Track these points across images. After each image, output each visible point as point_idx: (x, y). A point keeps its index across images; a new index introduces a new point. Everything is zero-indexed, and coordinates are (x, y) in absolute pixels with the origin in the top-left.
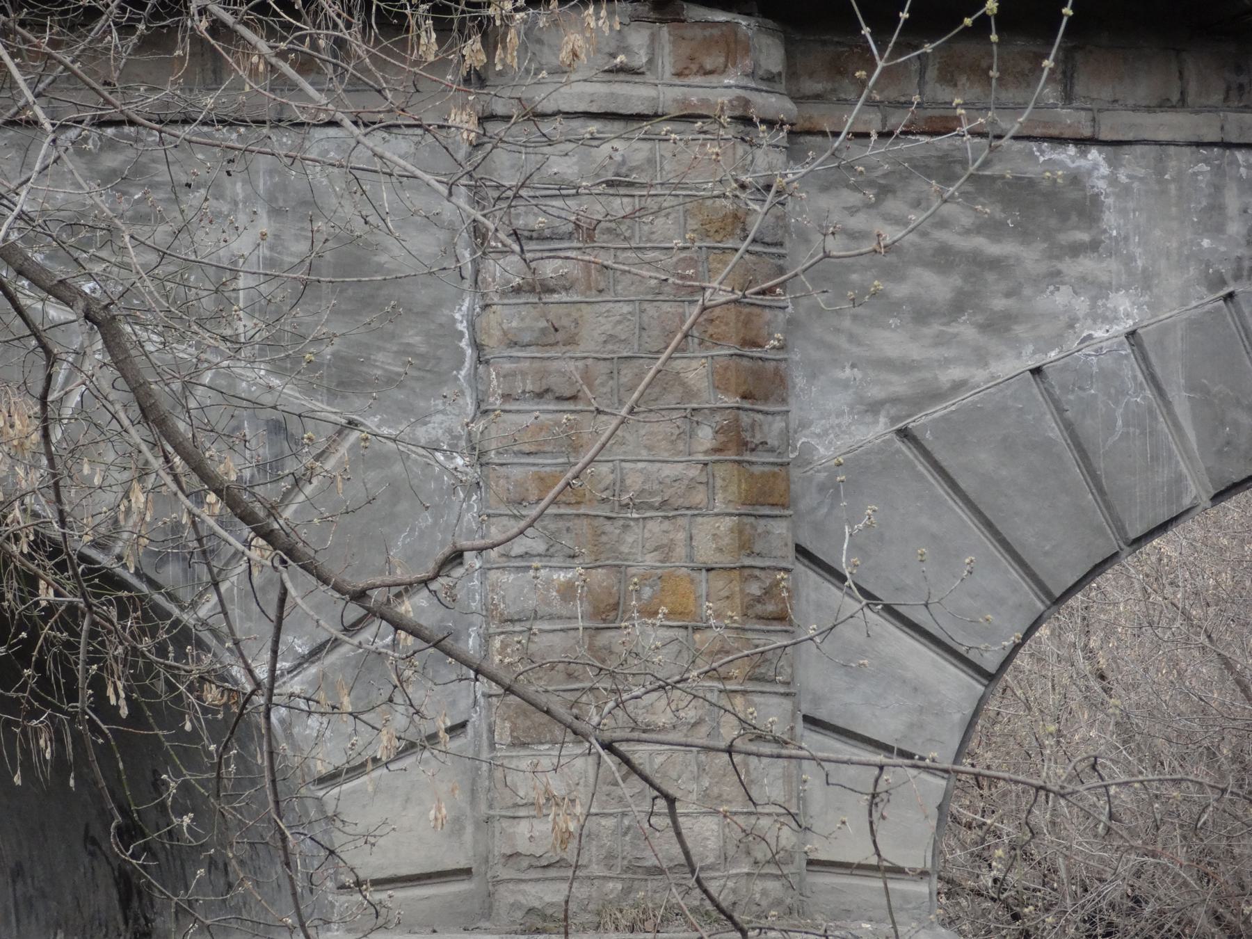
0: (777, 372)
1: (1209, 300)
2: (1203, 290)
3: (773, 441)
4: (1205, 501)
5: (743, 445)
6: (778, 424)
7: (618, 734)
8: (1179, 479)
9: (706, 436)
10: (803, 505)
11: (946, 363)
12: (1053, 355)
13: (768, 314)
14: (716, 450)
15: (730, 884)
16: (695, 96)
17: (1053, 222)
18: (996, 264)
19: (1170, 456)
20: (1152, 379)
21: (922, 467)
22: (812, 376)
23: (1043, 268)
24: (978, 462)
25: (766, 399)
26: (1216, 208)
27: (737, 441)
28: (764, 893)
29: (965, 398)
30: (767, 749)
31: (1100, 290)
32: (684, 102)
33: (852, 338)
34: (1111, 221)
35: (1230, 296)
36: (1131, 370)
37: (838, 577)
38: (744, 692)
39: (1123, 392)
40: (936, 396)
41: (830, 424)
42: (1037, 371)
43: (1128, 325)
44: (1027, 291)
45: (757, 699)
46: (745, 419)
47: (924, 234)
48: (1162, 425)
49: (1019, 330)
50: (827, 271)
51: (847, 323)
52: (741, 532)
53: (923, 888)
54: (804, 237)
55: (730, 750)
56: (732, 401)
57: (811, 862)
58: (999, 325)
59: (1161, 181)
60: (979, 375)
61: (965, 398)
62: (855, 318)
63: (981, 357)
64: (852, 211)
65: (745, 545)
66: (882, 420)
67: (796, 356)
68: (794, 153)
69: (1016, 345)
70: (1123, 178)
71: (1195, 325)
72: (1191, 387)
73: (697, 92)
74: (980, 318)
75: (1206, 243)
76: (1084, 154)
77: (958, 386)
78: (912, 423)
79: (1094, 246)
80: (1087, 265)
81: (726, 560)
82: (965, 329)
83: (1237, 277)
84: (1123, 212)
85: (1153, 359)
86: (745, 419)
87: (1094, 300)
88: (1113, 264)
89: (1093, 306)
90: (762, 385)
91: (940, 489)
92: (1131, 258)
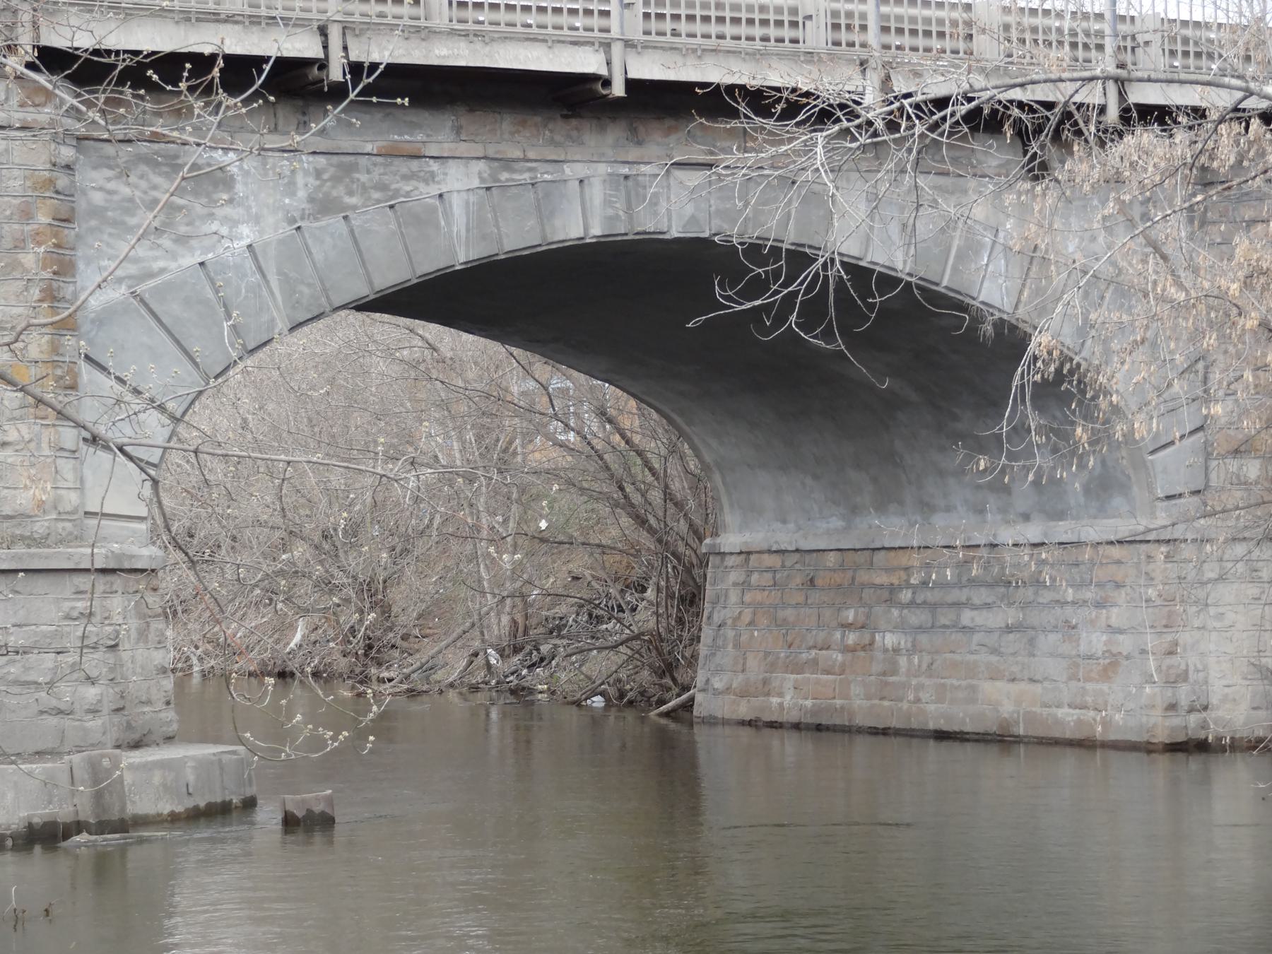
0: (71, 261)
1: (288, 230)
2: (285, 224)
3: (68, 297)
4: (286, 331)
5: (54, 298)
6: (71, 288)
7: (126, 440)
8: (273, 320)
9: (36, 293)
10: (83, 330)
11: (156, 259)
12: (210, 256)
13: (66, 231)
14: (40, 301)
15: (46, 524)
16: (30, 117)
17: (210, 188)
18: (180, 208)
19: (269, 309)
20: (260, 269)
21: (143, 311)
22: (88, 264)
23: (205, 211)
24: (172, 310)
25: (65, 275)
26: (292, 184)
27: (51, 296)
28: (64, 529)
29: (165, 277)
30: (66, 454)
31: (234, 223)
32: (24, 120)
33: (108, 245)
34: (240, 188)
35: (299, 228)
36: (249, 264)
37: (103, 369)
38: (54, 425)
39: (245, 275)
40: (151, 275)
41: (96, 289)
42: (202, 264)
43: (248, 241)
44: (197, 223)
45: (60, 429)
46: (55, 285)
47: (145, 193)
48: (265, 292)
49: (193, 242)
50: (96, 212)
51: (105, 237)
52: (52, 342)
53: (143, 526)
54: (84, 193)
55: (196, 452)
56: (47, 274)
57: (86, 513)
58: (182, 240)
59: (264, 169)
60: (173, 265)
61: (165, 277)
62: (110, 234)
63: (174, 257)
64: (109, 179)
65: (55, 349)
66: (124, 287)
67: (79, 253)
68: (78, 149)
69: (192, 250)
70: (246, 167)
71: (281, 242)
72: (280, 273)
73: (30, 116)
74: (173, 236)
75: (287, 201)
76: (226, 154)
77: (163, 271)
78: (139, 289)
79: (230, 201)
80: (228, 211)
81: (45, 357)
82: (166, 242)
83: (302, 218)
84: (246, 184)
85: (260, 259)
86: (55, 285)
87: (231, 228)
88: (241, 210)
89: (230, 231)
90: (63, 267)
91: (153, 323)
92: (249, 207)
